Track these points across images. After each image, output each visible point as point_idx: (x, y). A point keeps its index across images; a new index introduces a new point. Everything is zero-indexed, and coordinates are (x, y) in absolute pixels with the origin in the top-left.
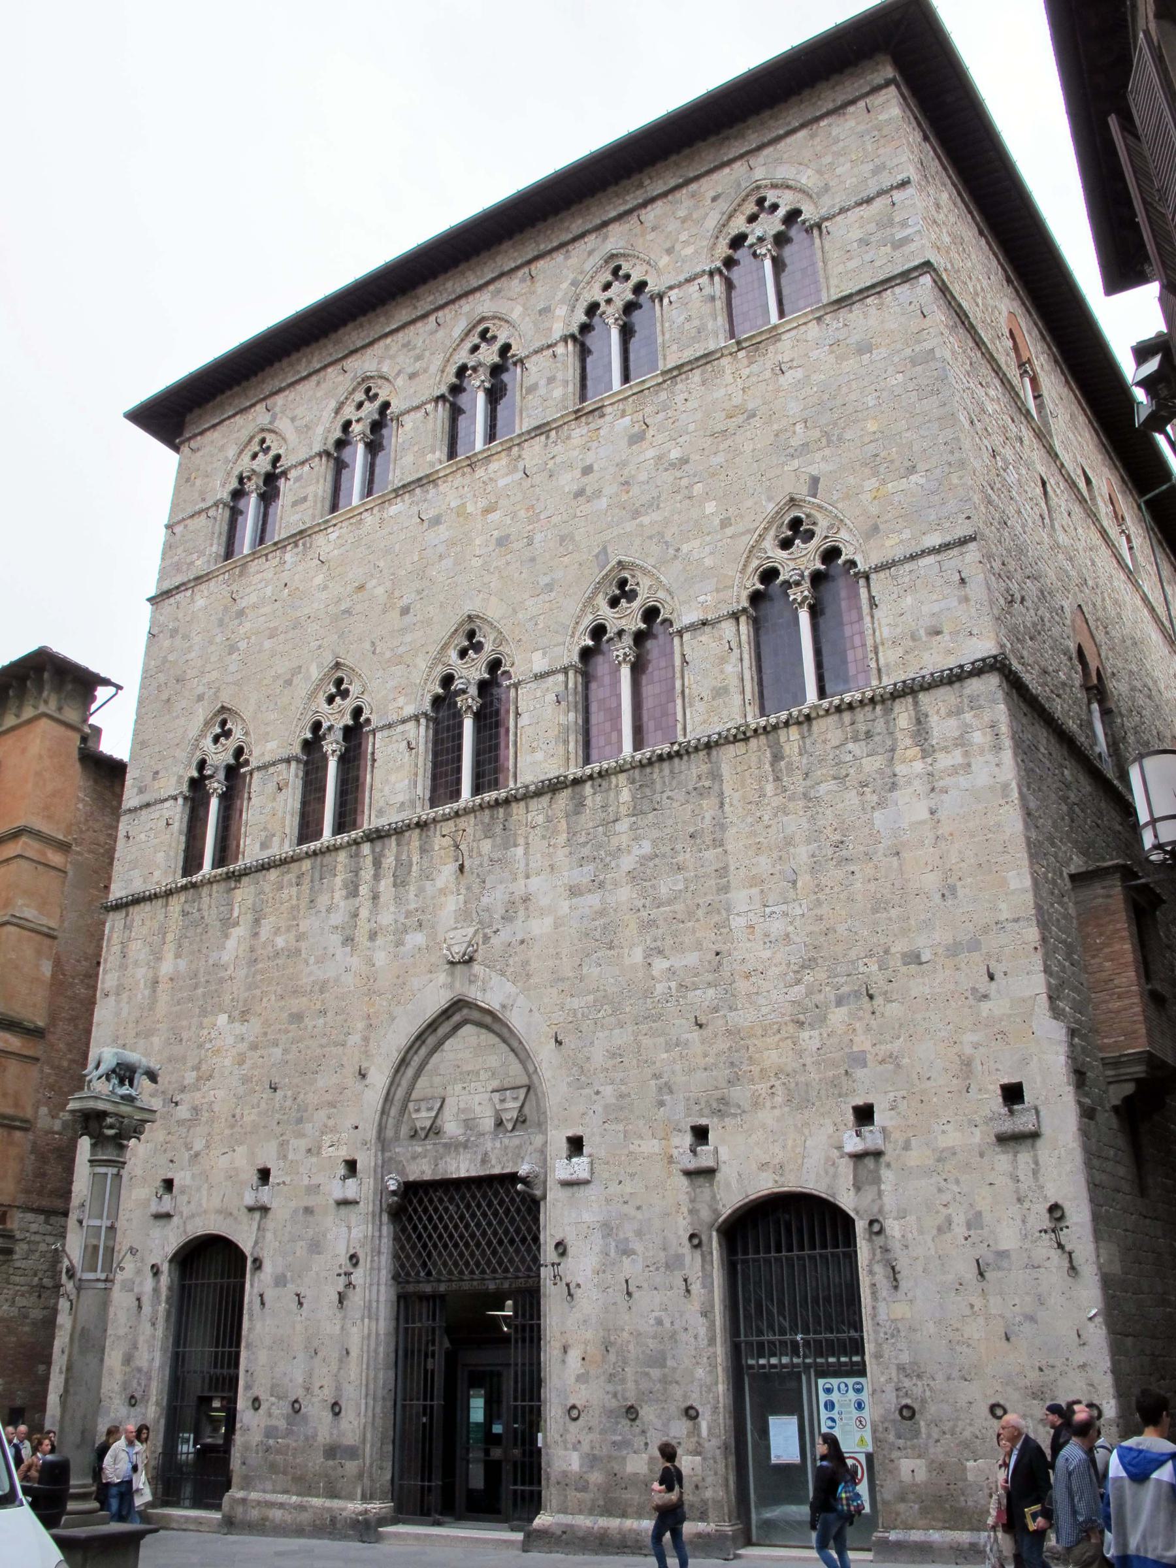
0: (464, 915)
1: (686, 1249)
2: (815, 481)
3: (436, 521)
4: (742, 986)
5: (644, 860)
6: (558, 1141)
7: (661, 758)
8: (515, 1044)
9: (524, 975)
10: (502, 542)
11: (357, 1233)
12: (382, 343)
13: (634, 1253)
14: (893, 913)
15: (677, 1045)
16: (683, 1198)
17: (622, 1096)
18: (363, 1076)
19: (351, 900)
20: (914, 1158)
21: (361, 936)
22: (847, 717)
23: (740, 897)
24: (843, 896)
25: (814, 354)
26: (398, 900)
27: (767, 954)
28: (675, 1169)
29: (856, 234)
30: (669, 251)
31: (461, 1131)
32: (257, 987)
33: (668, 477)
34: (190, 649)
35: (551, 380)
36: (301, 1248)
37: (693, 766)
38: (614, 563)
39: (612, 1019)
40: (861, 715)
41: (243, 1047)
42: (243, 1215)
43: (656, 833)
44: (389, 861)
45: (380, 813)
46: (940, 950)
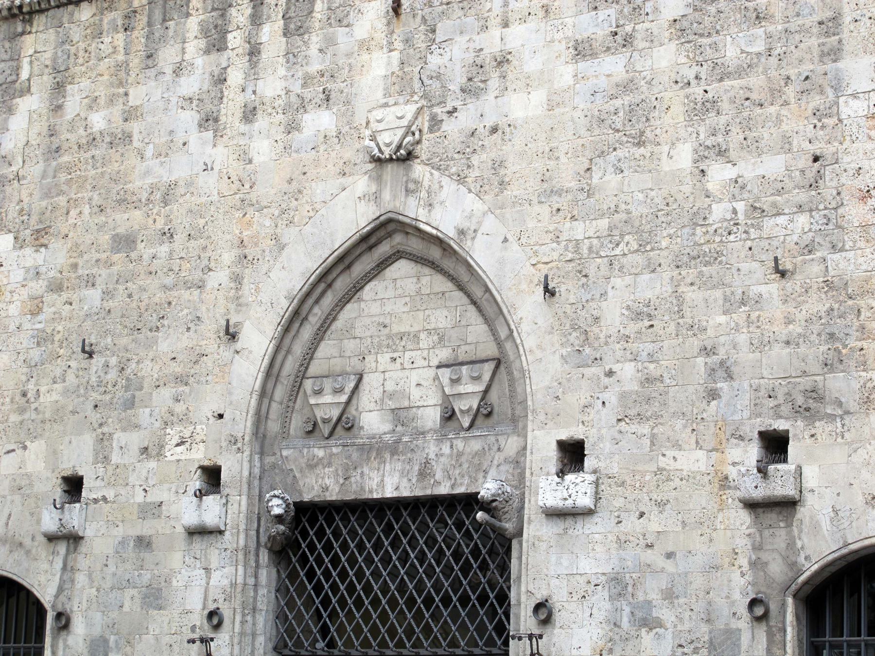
0: (400, 84)
1: (743, 623)
8: (478, 292)
9: (497, 180)
11: (221, 579)
13: (659, 623)
15: (743, 303)
16: (743, 543)
17: (649, 380)
19: (214, 56)
21: (231, 110)
26: (291, 56)
28: (732, 498)
31: (387, 427)
32: (61, 193)
36: (130, 600)
39: (639, 259)
41: (38, 287)
42: (41, 548)
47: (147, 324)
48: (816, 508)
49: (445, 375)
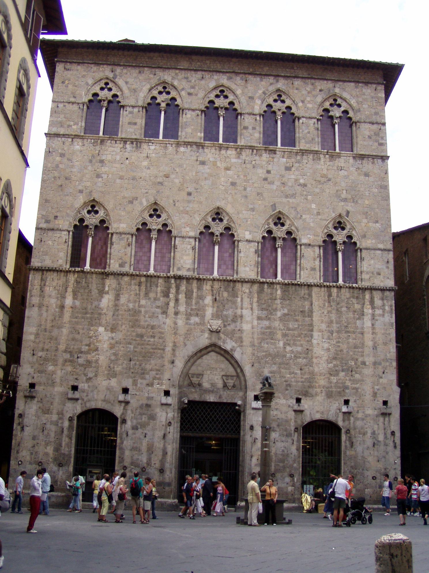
0: (216, 316)
2: (348, 213)
3: (203, 163)
4: (315, 360)
5: (285, 315)
6: (251, 395)
7: (293, 284)
8: (233, 362)
9: (240, 340)
10: (233, 184)
11: (170, 415)
12: (174, 71)
14: (360, 350)
16: (293, 418)
18: (173, 363)
20: (360, 415)
22: (351, 290)
23: (316, 334)
24: (346, 342)
25: (351, 169)
26: (188, 304)
27: (323, 353)
29: (367, 133)
30: (303, 102)
33: (299, 189)
34: (73, 166)
35: (254, 128)
36: (144, 419)
37: (303, 290)
38: (278, 210)
40: (356, 291)
41: (113, 342)
43: (289, 307)
44: (183, 288)
45: (179, 269)
46: (371, 363)
47: (147, 356)
48: (307, 413)
49: (224, 378)
